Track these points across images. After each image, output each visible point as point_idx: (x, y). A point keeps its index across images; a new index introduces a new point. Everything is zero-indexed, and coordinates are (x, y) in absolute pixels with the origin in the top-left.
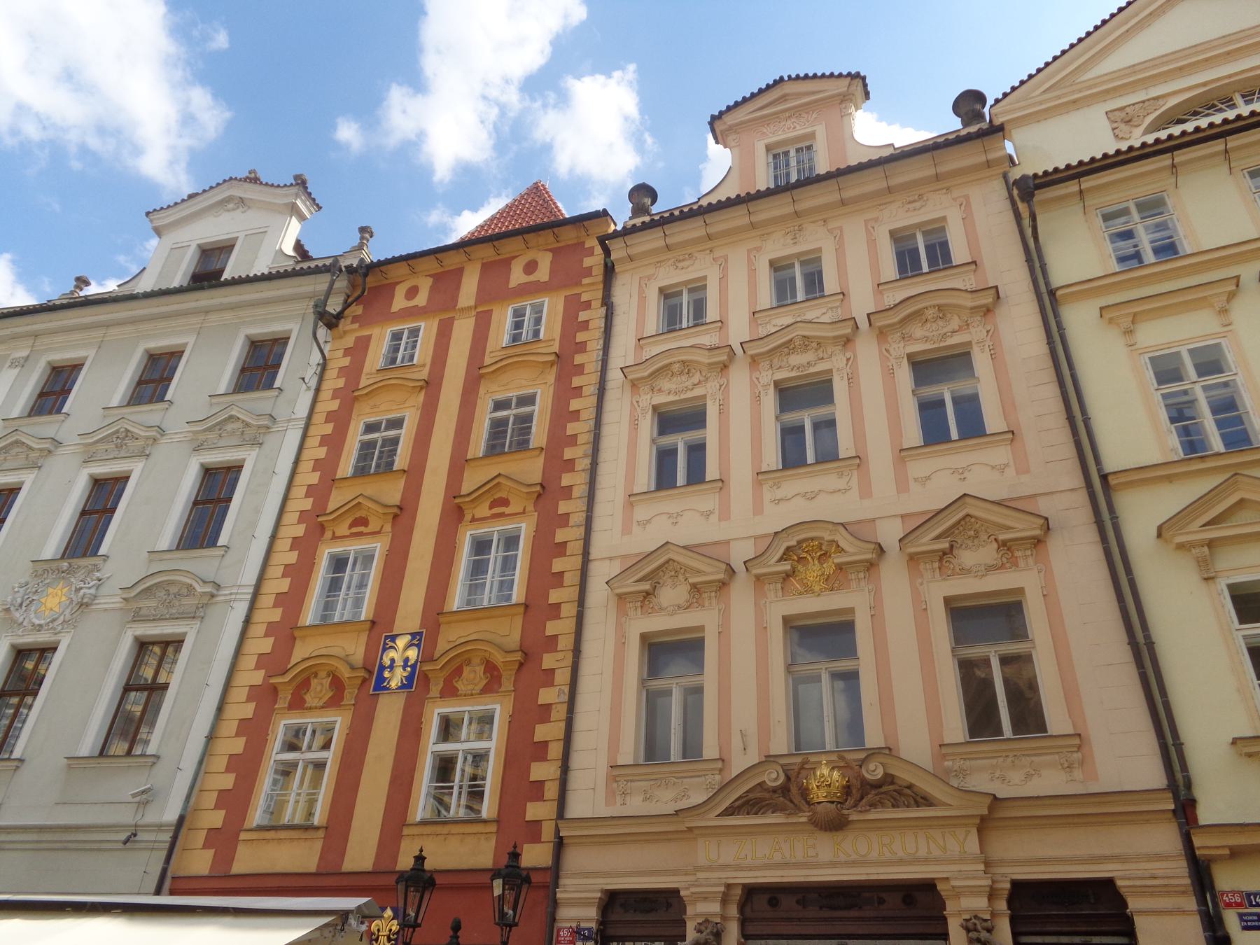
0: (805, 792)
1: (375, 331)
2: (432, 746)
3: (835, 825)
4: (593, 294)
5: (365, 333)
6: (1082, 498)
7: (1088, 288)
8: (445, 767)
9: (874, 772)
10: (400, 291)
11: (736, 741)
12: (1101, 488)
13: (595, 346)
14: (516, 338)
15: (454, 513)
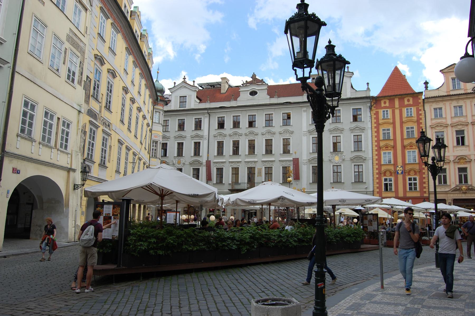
0: (462, 189)
1: (379, 110)
2: (408, 182)
3: (465, 193)
4: (421, 108)
5: (377, 110)
8: (410, 184)
9: (470, 188)
10: (382, 102)
11: (452, 183)
13: (423, 119)
14: (407, 115)
15: (404, 147)
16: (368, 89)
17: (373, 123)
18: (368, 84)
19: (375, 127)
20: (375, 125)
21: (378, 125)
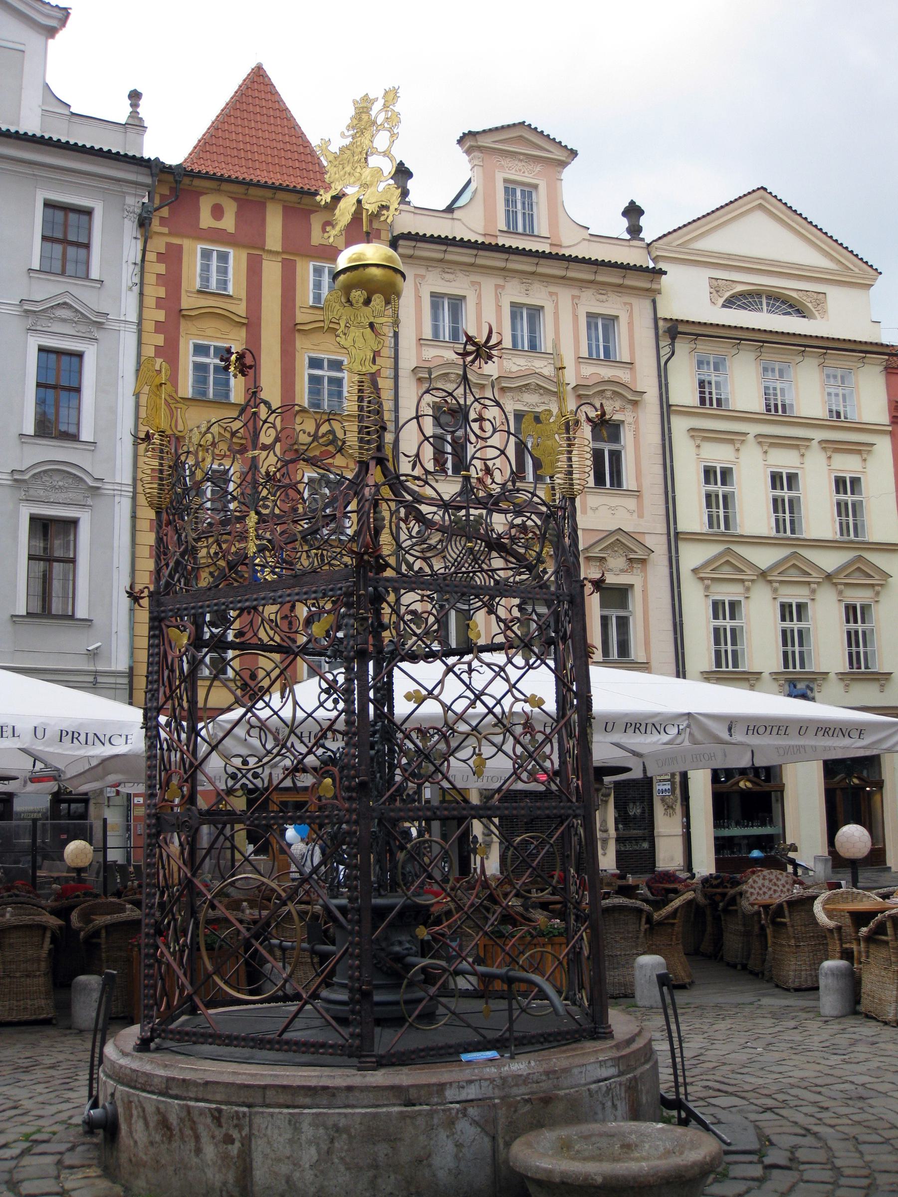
1: (186, 243)
5: (176, 241)
6: (665, 538)
7: (686, 412)
10: (206, 205)
12: (675, 537)
16: (136, 124)
17: (150, 302)
18: (135, 96)
19: (159, 327)
20: (161, 316)
21: (175, 316)
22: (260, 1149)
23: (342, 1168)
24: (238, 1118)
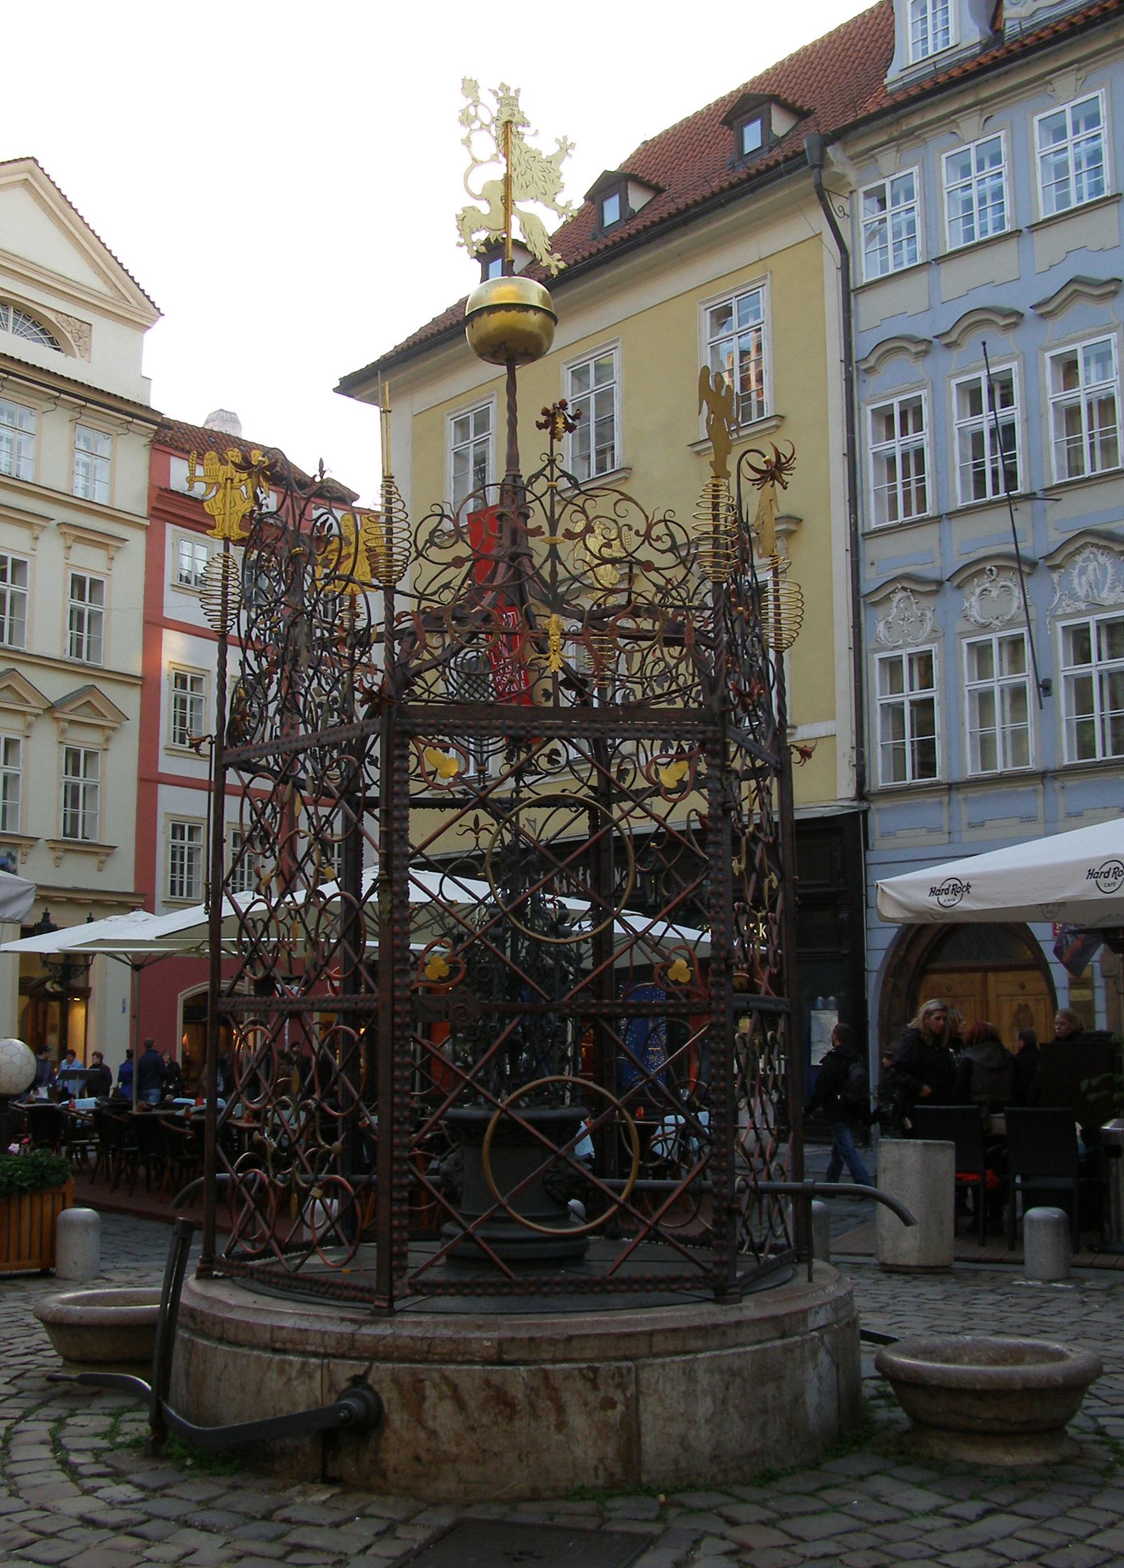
22: (650, 1408)
23: (736, 1417)
24: (621, 1375)
